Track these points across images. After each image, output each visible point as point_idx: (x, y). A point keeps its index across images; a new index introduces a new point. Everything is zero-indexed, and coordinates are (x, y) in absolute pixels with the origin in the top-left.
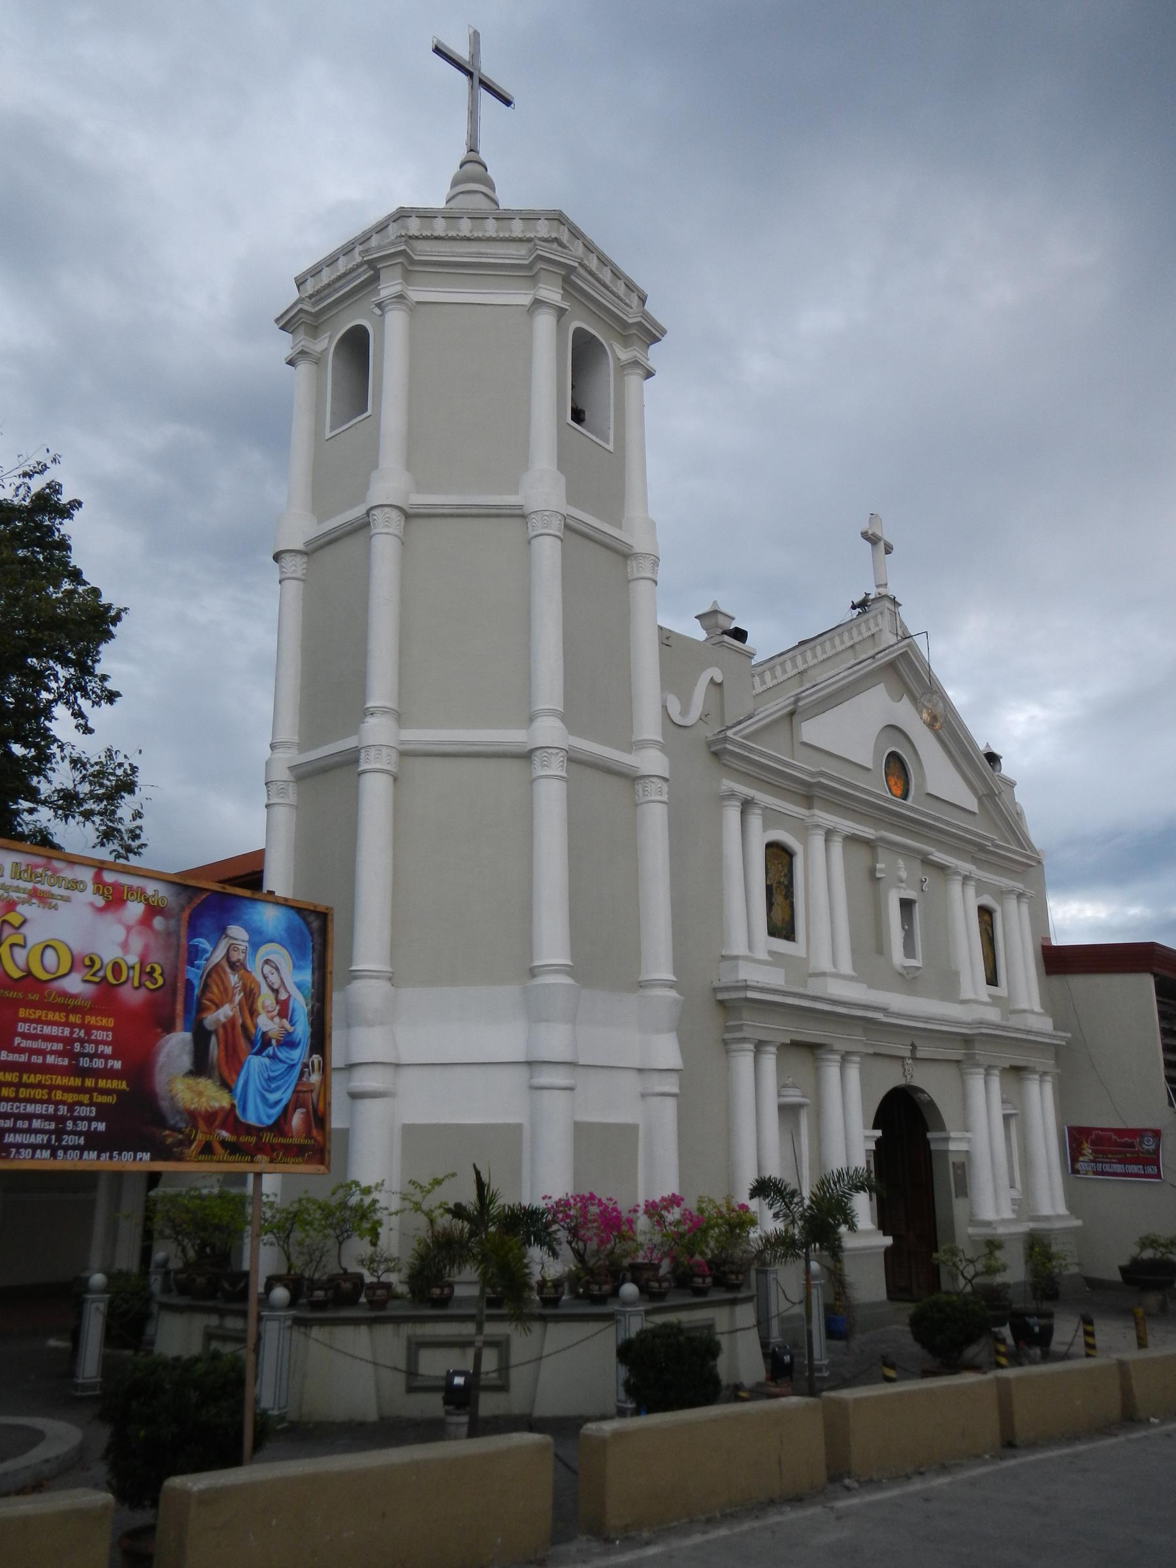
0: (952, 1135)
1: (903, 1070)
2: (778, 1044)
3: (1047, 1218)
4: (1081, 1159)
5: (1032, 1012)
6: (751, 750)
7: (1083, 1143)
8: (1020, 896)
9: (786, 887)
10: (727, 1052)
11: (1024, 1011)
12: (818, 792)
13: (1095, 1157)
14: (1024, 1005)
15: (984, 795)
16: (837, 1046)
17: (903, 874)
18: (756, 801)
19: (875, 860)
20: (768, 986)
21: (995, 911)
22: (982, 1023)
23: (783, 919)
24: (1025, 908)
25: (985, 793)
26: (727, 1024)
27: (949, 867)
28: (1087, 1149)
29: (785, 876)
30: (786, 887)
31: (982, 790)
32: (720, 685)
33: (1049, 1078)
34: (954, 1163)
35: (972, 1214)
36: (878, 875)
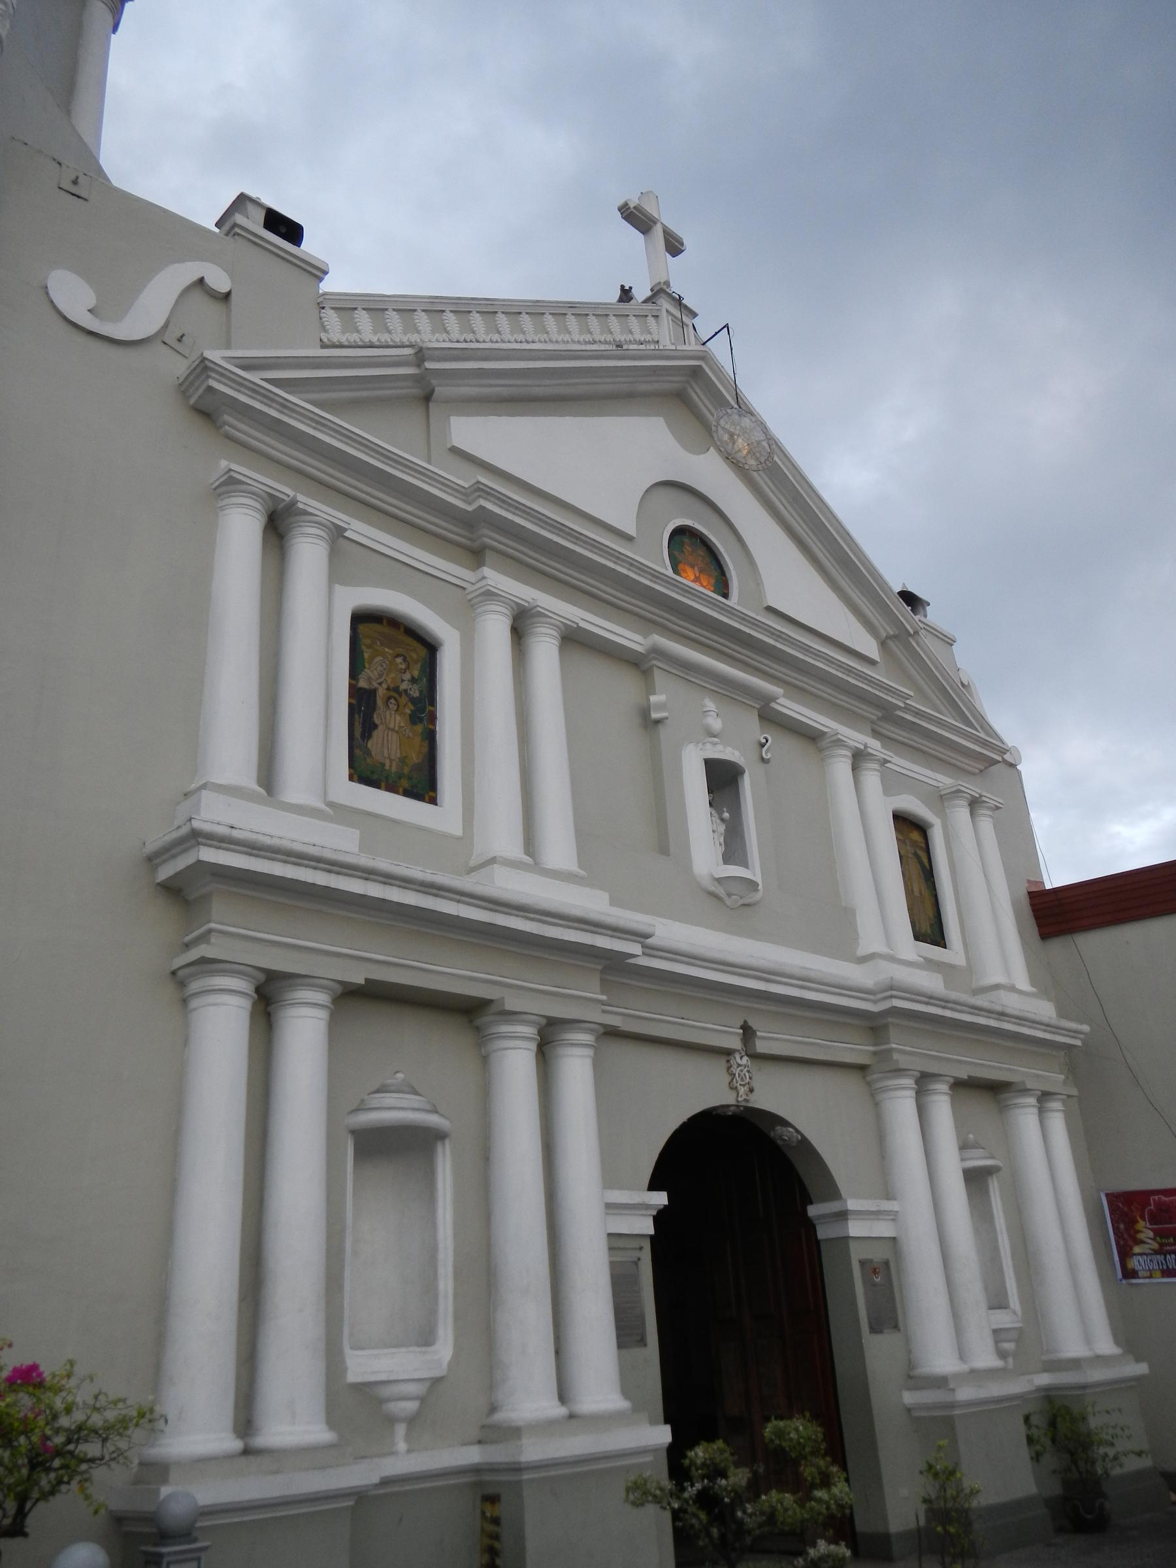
0: (852, 1204)
1: (727, 1078)
2: (339, 989)
3: (1075, 1364)
4: (1137, 1249)
5: (1012, 989)
6: (285, 406)
7: (1135, 1222)
8: (974, 804)
9: (413, 700)
10: (185, 1001)
11: (997, 987)
12: (489, 538)
13: (1161, 1245)
14: (997, 978)
15: (889, 637)
16: (511, 1004)
17: (716, 724)
18: (300, 506)
19: (650, 689)
20: (268, 841)
21: (931, 826)
22: (892, 988)
23: (403, 760)
24: (986, 825)
25: (892, 633)
26: (187, 939)
27: (824, 733)
28: (1145, 1231)
29: (413, 680)
30: (413, 700)
31: (886, 629)
32: (227, 296)
33: (1056, 1105)
34: (863, 1263)
35: (911, 1364)
36: (655, 715)
